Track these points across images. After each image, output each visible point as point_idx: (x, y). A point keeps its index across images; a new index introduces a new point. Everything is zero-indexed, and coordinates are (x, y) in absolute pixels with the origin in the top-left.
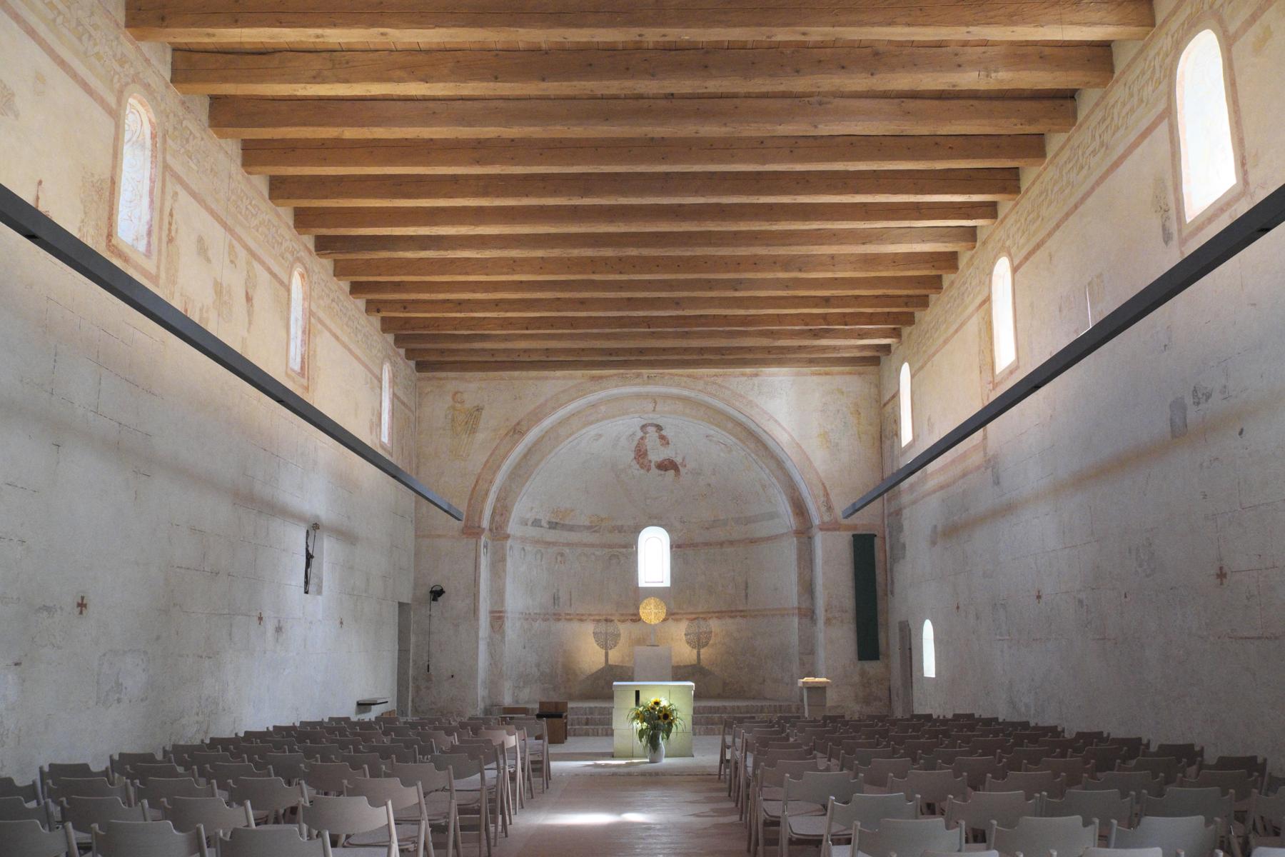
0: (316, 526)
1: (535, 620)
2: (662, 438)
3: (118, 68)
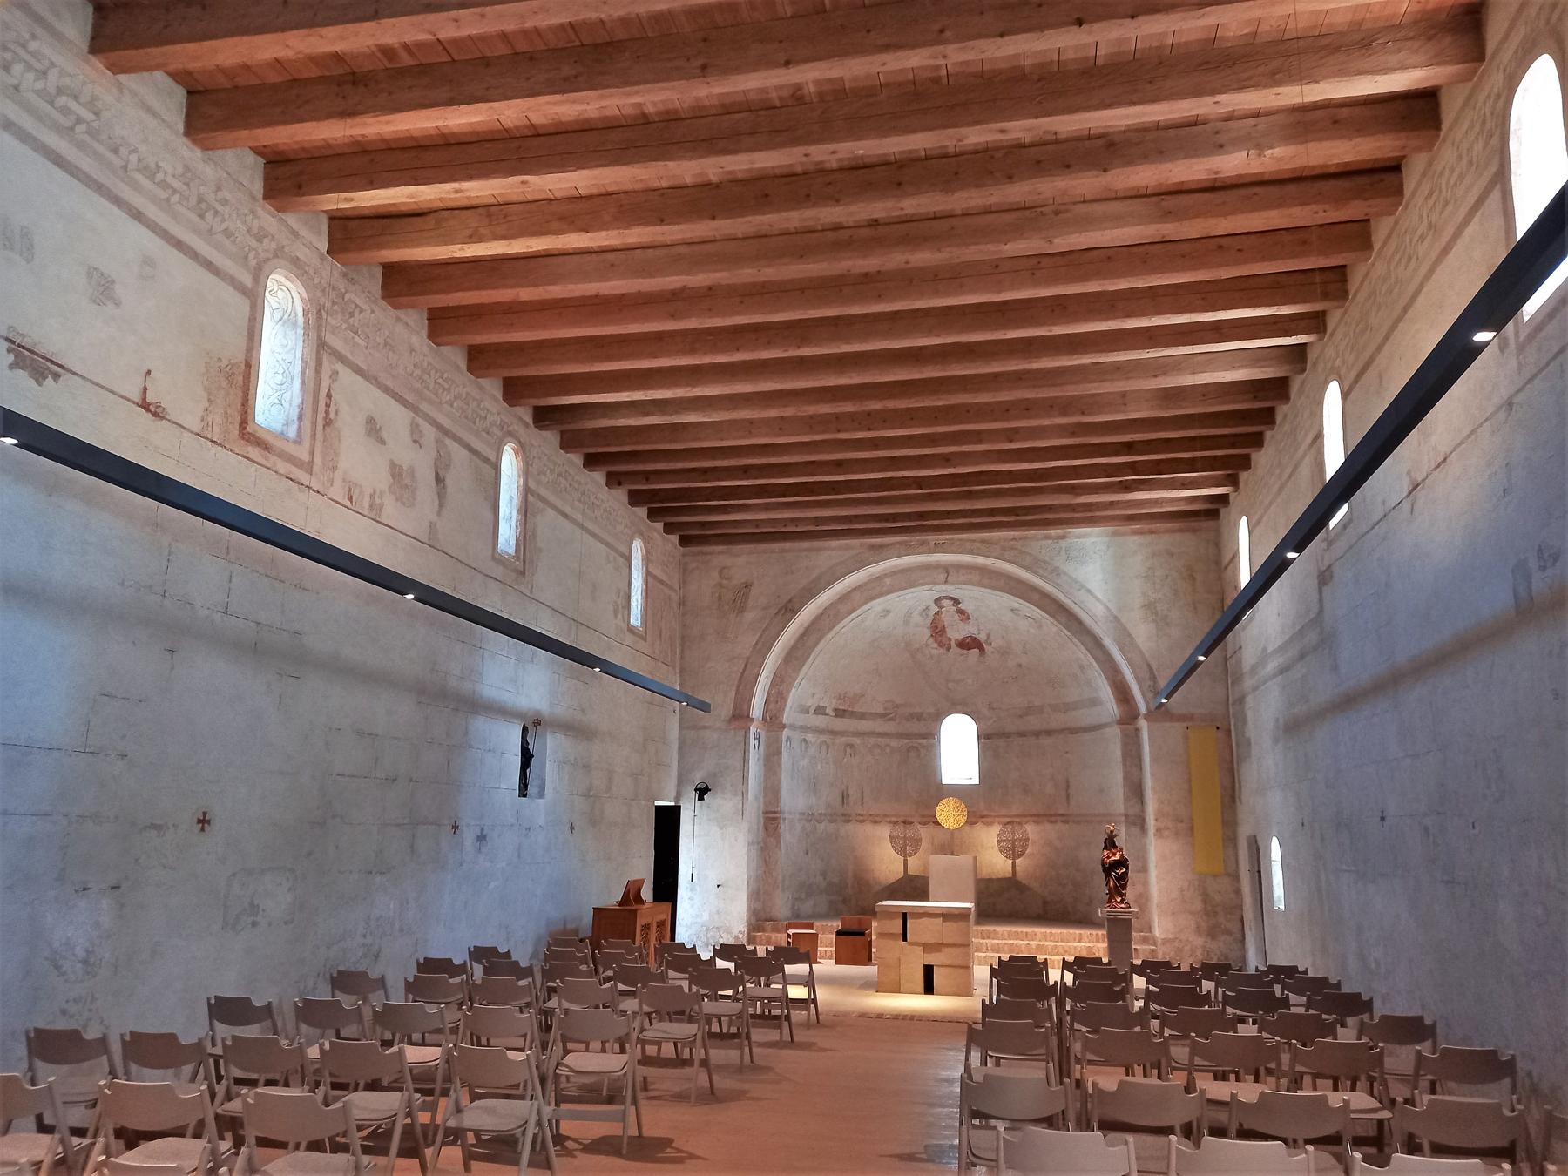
0: (537, 723)
1: (819, 822)
2: (961, 612)
3: (254, 243)
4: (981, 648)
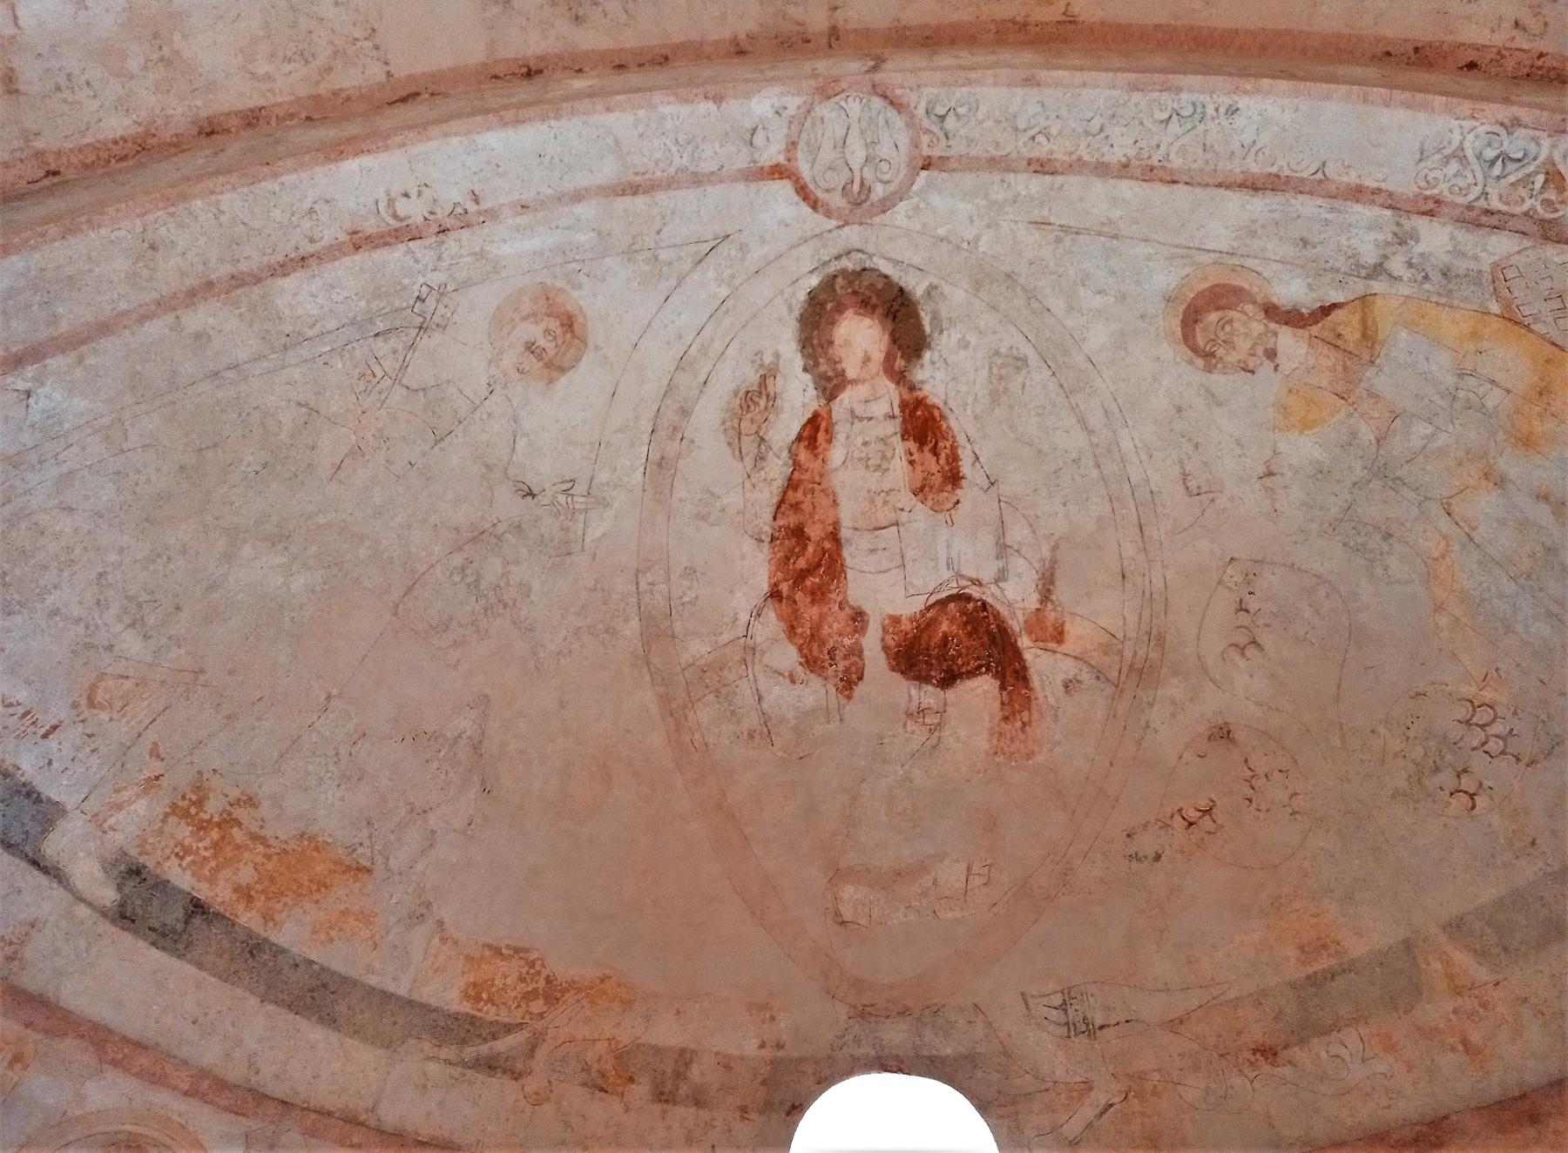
2: (922, 425)
4: (1010, 669)
